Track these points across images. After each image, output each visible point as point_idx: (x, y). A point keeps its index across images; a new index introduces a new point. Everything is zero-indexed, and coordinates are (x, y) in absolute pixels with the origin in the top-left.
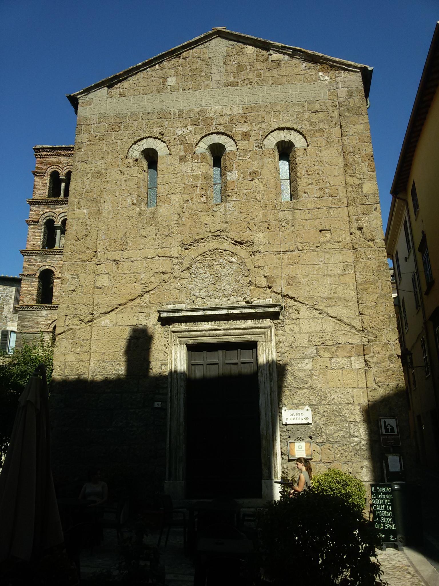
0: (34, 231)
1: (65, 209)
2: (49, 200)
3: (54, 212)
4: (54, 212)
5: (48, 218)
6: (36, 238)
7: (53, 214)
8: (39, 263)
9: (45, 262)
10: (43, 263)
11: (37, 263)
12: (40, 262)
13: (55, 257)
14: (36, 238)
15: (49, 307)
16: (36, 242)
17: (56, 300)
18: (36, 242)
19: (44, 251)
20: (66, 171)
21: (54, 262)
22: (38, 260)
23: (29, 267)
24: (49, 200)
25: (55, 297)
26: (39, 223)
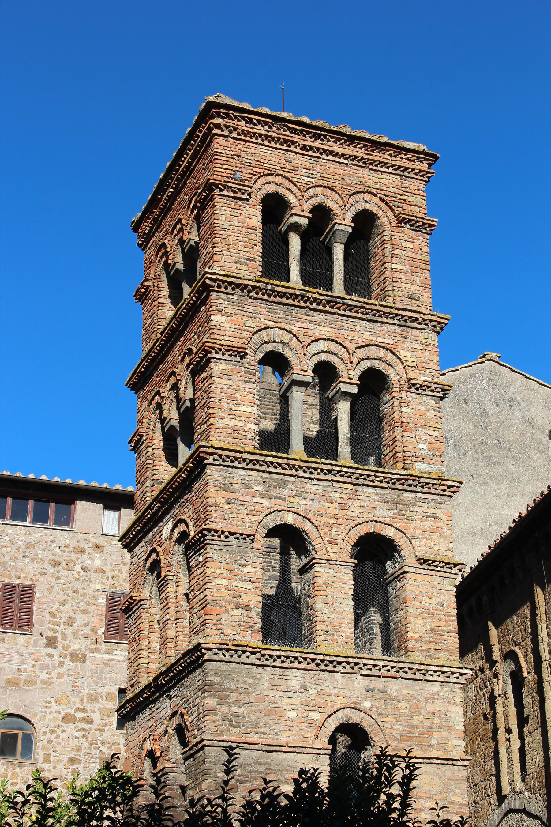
0: (230, 383)
1: (324, 329)
2: (277, 288)
3: (290, 332)
4: (290, 332)
5: (269, 348)
6: (241, 408)
7: (287, 337)
8: (258, 500)
9: (279, 498)
10: (273, 501)
11: (255, 500)
12: (262, 496)
13: (310, 486)
14: (241, 408)
15: (313, 660)
16: (241, 424)
17: (329, 638)
18: (241, 424)
19: (280, 461)
20: (310, 201)
21: (308, 502)
22: (256, 488)
23: (226, 506)
24: (277, 288)
25: (325, 628)
26: (246, 360)
